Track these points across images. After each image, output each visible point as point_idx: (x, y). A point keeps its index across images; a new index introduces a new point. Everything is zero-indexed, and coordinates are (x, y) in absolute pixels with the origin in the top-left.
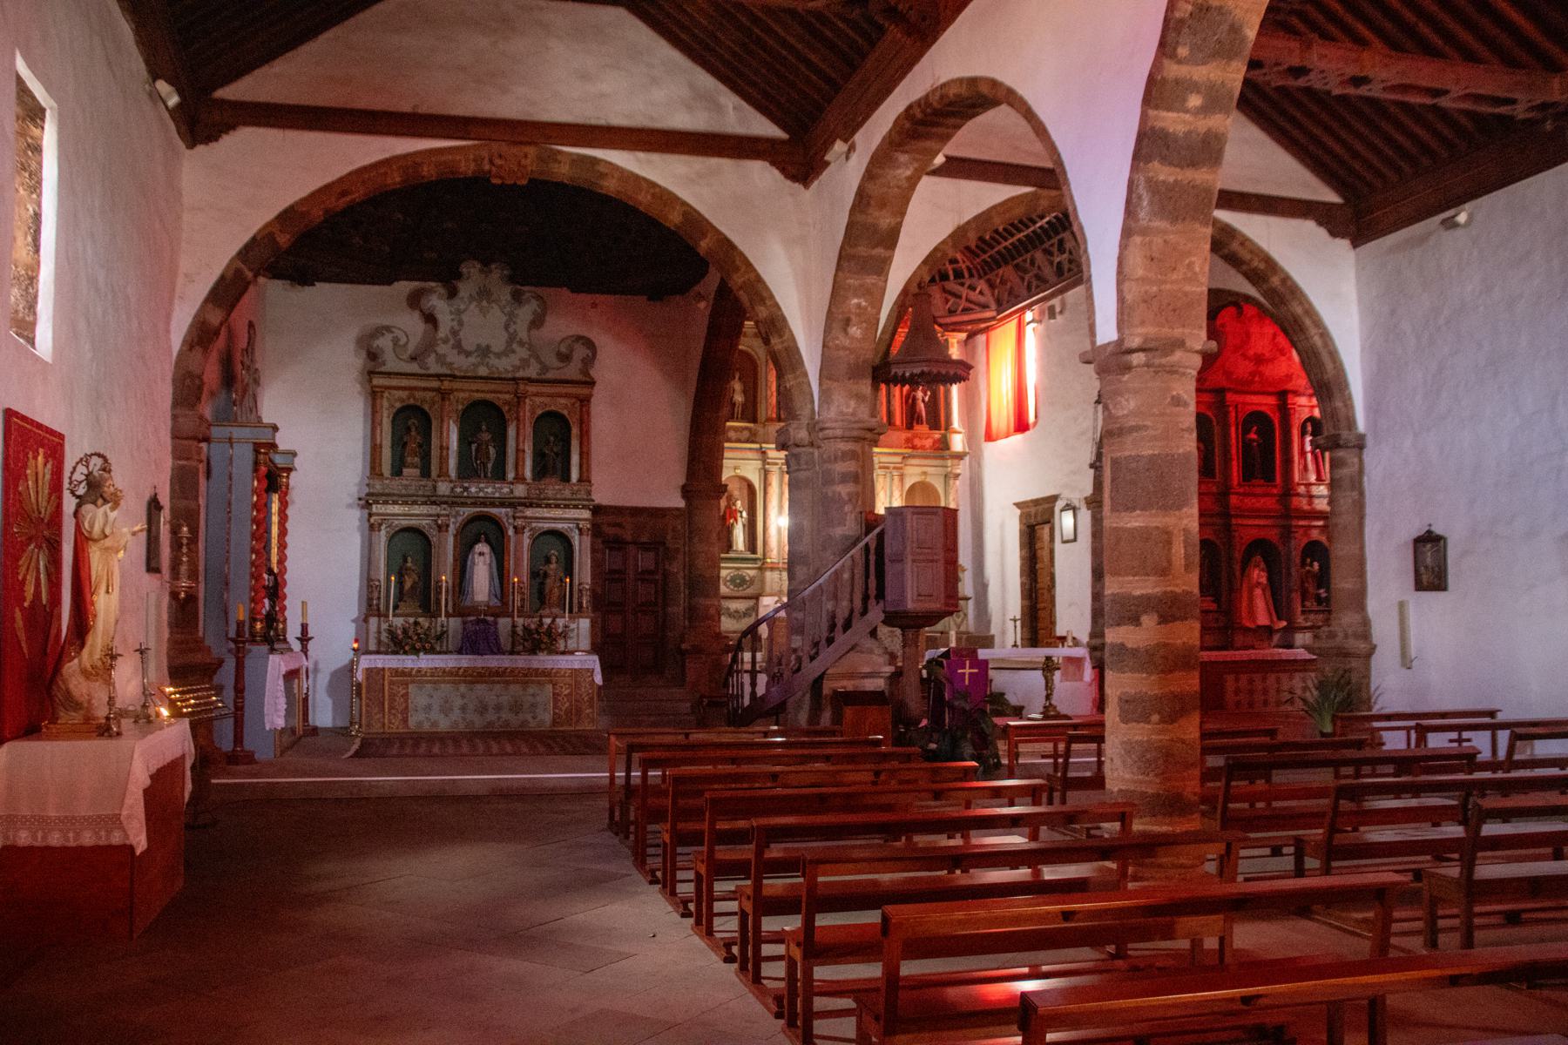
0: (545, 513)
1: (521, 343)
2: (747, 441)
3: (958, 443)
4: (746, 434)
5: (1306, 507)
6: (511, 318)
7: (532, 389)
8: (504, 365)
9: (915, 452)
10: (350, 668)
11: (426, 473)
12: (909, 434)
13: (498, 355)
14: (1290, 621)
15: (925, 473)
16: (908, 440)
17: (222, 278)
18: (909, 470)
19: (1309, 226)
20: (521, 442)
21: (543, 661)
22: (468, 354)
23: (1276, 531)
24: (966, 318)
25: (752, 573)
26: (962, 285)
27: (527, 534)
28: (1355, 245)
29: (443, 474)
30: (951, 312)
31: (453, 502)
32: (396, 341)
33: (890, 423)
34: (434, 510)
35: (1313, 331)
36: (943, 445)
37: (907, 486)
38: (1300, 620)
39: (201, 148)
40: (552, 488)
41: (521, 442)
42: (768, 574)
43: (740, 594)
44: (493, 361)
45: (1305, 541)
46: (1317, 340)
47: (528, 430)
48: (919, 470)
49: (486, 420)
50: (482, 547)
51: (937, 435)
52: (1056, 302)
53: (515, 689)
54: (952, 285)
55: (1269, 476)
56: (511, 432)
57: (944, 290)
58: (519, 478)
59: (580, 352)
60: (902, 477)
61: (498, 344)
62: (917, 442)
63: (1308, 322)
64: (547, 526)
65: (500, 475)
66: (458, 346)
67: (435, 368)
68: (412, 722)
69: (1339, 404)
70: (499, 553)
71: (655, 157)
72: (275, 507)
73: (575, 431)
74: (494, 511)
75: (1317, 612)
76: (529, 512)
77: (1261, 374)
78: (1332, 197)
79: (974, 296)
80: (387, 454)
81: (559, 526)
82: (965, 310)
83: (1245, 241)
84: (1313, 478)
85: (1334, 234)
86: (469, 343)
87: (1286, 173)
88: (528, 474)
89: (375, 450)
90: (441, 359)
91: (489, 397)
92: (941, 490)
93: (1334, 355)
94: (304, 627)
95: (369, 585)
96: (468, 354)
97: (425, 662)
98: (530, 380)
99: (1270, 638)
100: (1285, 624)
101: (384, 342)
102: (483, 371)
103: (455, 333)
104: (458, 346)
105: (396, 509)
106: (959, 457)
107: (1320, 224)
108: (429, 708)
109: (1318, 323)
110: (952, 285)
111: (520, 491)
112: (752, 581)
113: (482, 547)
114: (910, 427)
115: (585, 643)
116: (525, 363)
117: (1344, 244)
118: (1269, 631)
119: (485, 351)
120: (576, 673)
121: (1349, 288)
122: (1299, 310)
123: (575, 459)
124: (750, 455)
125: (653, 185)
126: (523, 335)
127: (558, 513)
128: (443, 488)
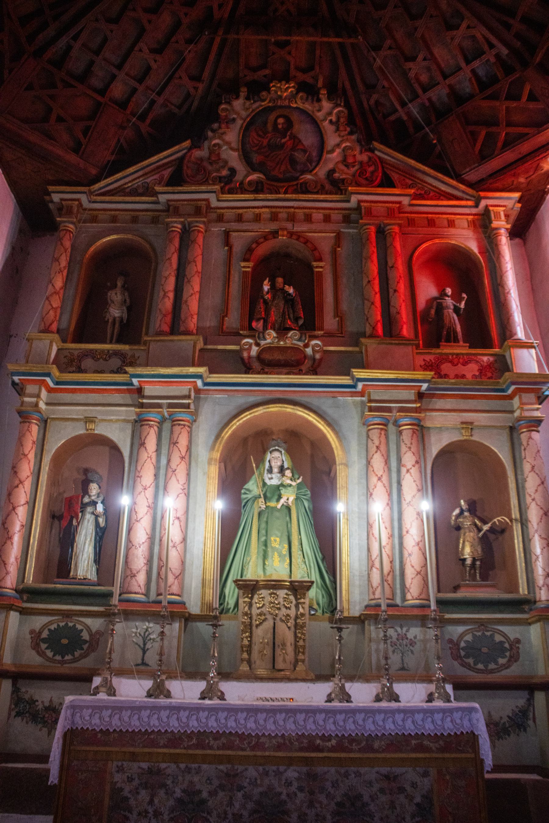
9: (442, 383)
15: (468, 425)
18: (434, 420)
24: (510, 156)
25: (95, 624)
26: (494, 97)
36: (503, 366)
42: (120, 627)
43: (65, 669)
48: (454, 419)
60: (421, 432)
92: (504, 456)
112: (97, 640)
124: (117, 398)
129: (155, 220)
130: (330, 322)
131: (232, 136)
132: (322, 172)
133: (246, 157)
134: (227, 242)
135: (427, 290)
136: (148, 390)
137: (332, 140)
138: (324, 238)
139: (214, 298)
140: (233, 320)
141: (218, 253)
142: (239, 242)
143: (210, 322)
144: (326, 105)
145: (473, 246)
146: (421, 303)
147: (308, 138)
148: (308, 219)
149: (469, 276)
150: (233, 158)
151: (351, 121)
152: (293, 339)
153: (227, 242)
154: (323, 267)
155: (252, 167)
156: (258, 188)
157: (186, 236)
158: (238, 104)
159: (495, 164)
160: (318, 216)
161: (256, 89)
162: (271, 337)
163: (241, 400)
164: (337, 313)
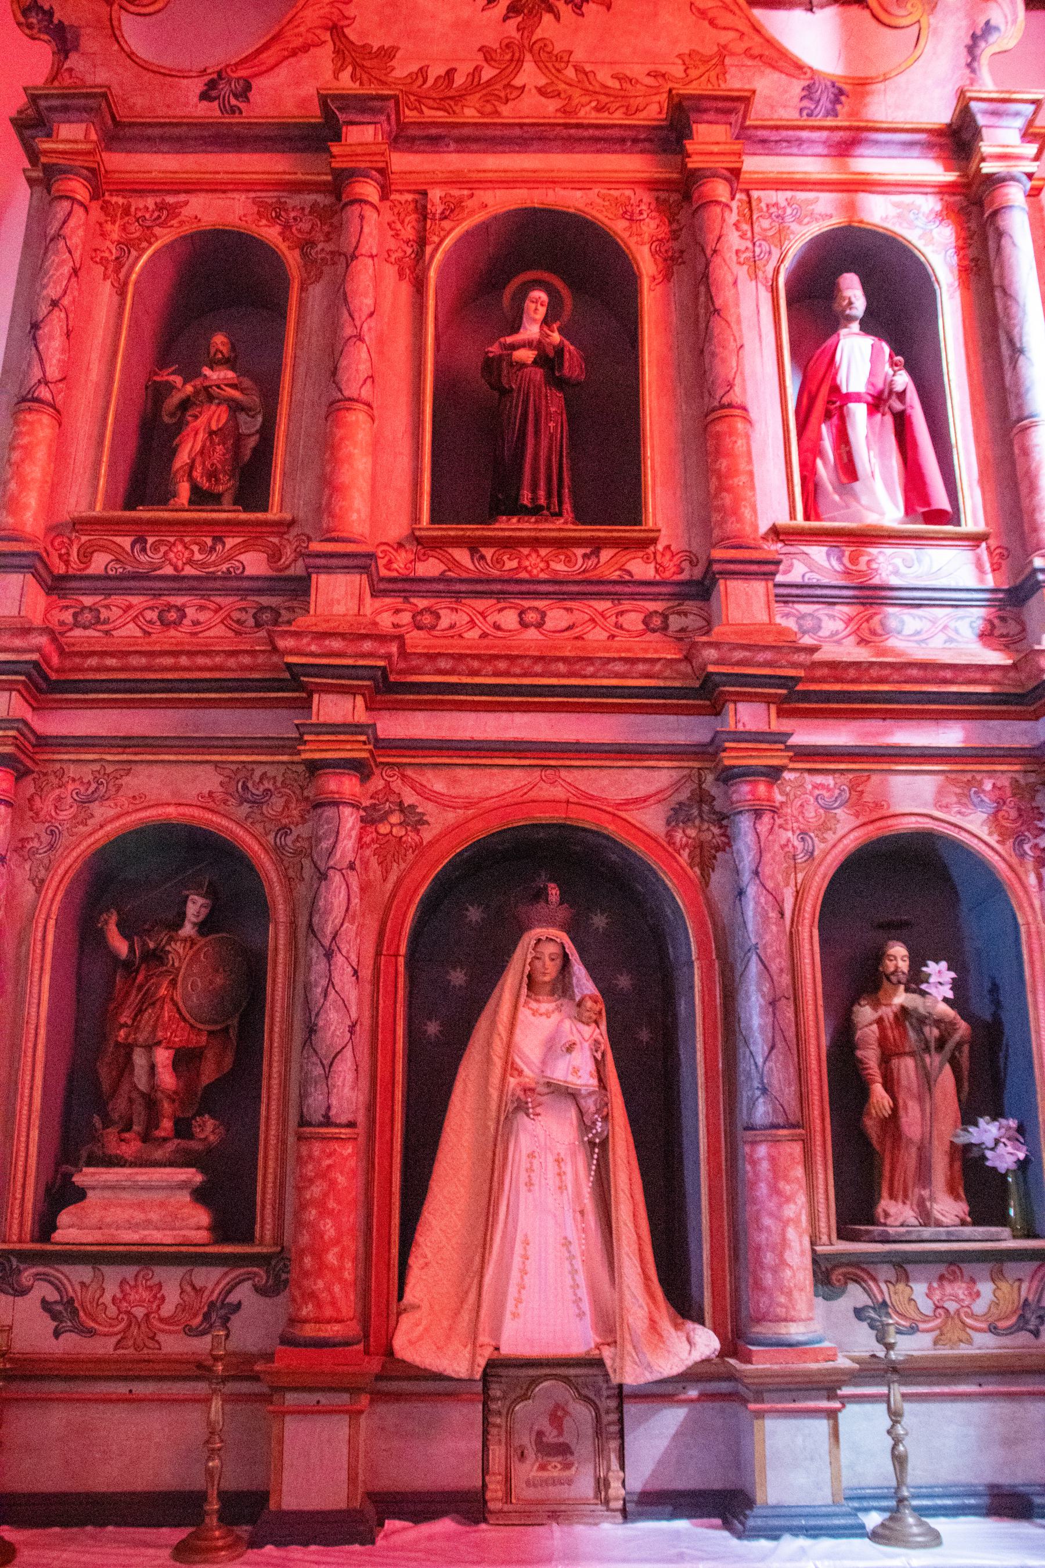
5: (851, 652)
14: (735, 1343)
23: (661, 777)
38: (820, 1326)
45: (845, 834)
55: (610, 494)
75: (953, 1265)
77: (551, 60)
84: (881, 502)
99: (611, 1434)
100: (706, 1342)
118: (594, 1394)
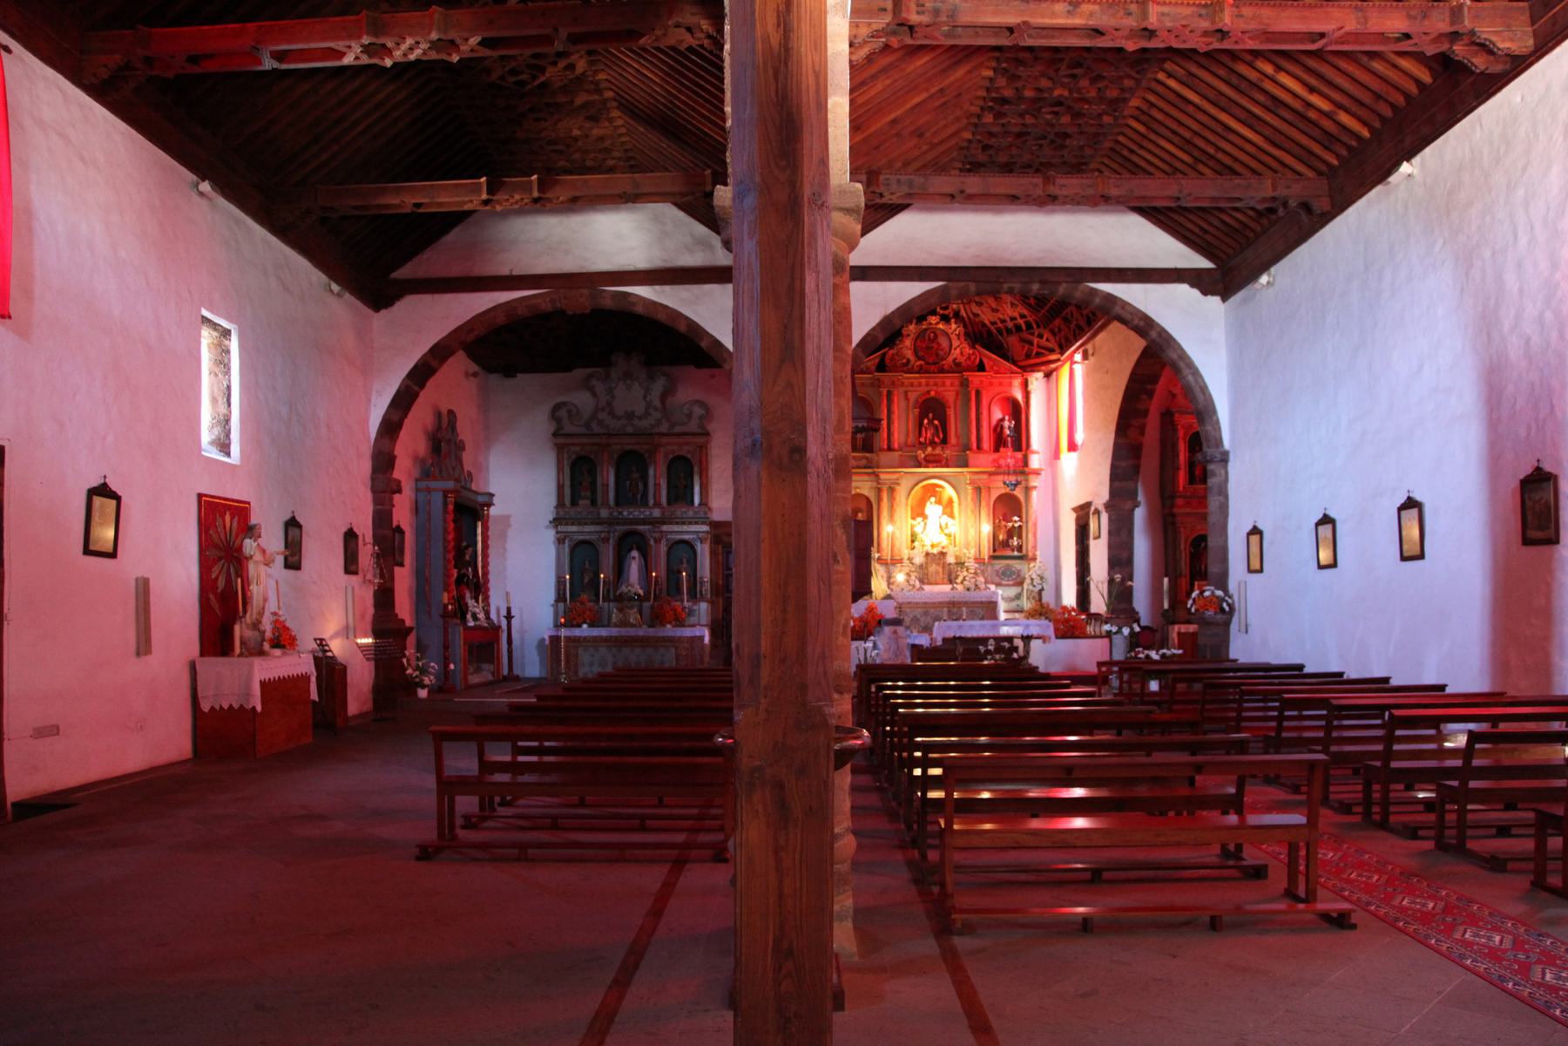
0: (676, 528)
1: (656, 409)
2: (865, 467)
3: (1035, 462)
4: (864, 462)
6: (648, 391)
7: (664, 440)
8: (644, 424)
10: (555, 640)
11: (594, 502)
12: (996, 455)
13: (640, 418)
16: (995, 461)
17: (398, 391)
19: (1183, 289)
20: (657, 476)
21: (669, 630)
22: (619, 418)
27: (663, 543)
28: (1224, 299)
29: (606, 504)
30: (1028, 356)
31: (611, 522)
32: (569, 412)
33: (979, 448)
34: (598, 528)
35: (1186, 371)
37: (994, 497)
39: (383, 312)
40: (681, 510)
41: (657, 476)
44: (636, 422)
46: (1190, 378)
47: (663, 469)
49: (632, 464)
50: (635, 553)
51: (1019, 455)
52: (1089, 347)
53: (650, 651)
54: (1025, 335)
56: (651, 472)
57: (1022, 340)
58: (657, 504)
59: (698, 411)
61: (640, 409)
62: (1002, 462)
63: (1182, 365)
64: (679, 537)
65: (645, 503)
66: (612, 414)
67: (597, 429)
68: (581, 674)
69: (1209, 428)
70: (645, 555)
71: (667, 288)
72: (479, 531)
73: (696, 469)
74: (641, 528)
76: (665, 528)
78: (1204, 263)
79: (1043, 342)
80: (567, 491)
81: (686, 537)
82: (1038, 355)
83: (1125, 304)
85: (1205, 292)
86: (619, 412)
87: (1168, 250)
88: (664, 500)
89: (560, 488)
90: (600, 423)
91: (636, 447)
93: (1204, 389)
94: (509, 609)
95: (560, 582)
96: (619, 418)
97: (585, 630)
98: (661, 435)
101: (563, 413)
102: (630, 430)
103: (609, 404)
104: (612, 414)
105: (574, 528)
106: (1037, 473)
107: (1192, 286)
108: (591, 664)
109: (1190, 365)
110: (1025, 335)
111: (657, 513)
113: (635, 553)
114: (997, 450)
115: (705, 619)
116: (659, 422)
117: (1215, 301)
119: (630, 416)
120: (693, 639)
121: (1219, 334)
122: (1174, 356)
123: (697, 489)
125: (666, 307)
126: (657, 403)
127: (685, 528)
128: (604, 513)
129: (872, 385)
130: (953, 440)
131: (908, 342)
132: (950, 359)
133: (915, 353)
134: (907, 399)
135: (997, 414)
136: (882, 477)
137: (955, 343)
138: (950, 396)
139: (904, 430)
140: (911, 439)
141: (903, 404)
142: (913, 396)
143: (902, 440)
144: (954, 326)
145: (1019, 396)
146: (994, 422)
147: (944, 342)
148: (944, 384)
149: (1018, 412)
150: (909, 354)
151: (967, 334)
152: (938, 451)
153: (907, 399)
154: (951, 412)
155: (919, 358)
156: (920, 370)
157: (889, 394)
158: (912, 327)
159: (1032, 361)
160: (948, 382)
161: (921, 319)
162: (929, 449)
163: (917, 478)
164: (957, 436)
